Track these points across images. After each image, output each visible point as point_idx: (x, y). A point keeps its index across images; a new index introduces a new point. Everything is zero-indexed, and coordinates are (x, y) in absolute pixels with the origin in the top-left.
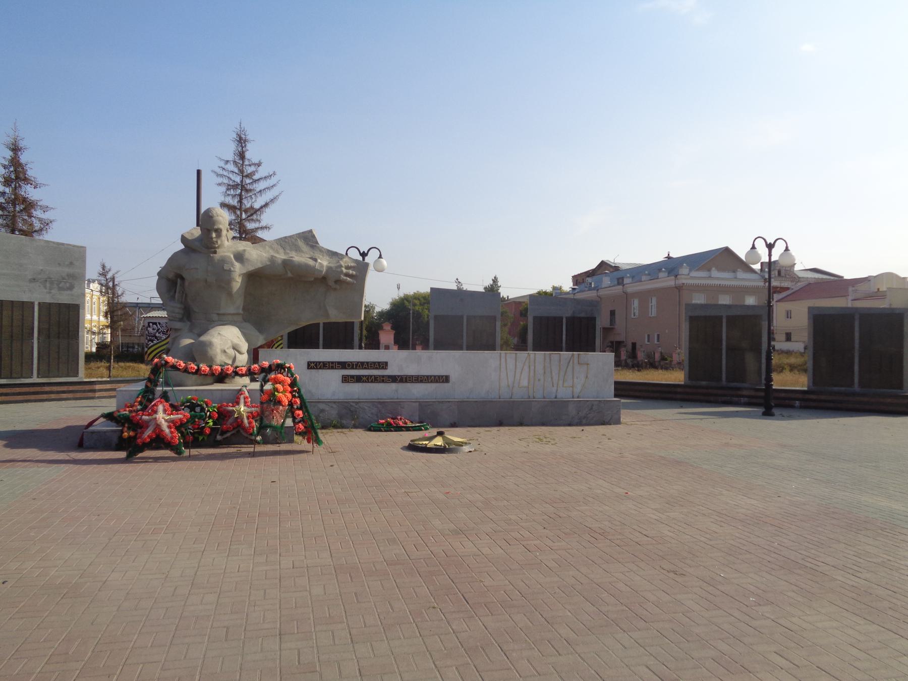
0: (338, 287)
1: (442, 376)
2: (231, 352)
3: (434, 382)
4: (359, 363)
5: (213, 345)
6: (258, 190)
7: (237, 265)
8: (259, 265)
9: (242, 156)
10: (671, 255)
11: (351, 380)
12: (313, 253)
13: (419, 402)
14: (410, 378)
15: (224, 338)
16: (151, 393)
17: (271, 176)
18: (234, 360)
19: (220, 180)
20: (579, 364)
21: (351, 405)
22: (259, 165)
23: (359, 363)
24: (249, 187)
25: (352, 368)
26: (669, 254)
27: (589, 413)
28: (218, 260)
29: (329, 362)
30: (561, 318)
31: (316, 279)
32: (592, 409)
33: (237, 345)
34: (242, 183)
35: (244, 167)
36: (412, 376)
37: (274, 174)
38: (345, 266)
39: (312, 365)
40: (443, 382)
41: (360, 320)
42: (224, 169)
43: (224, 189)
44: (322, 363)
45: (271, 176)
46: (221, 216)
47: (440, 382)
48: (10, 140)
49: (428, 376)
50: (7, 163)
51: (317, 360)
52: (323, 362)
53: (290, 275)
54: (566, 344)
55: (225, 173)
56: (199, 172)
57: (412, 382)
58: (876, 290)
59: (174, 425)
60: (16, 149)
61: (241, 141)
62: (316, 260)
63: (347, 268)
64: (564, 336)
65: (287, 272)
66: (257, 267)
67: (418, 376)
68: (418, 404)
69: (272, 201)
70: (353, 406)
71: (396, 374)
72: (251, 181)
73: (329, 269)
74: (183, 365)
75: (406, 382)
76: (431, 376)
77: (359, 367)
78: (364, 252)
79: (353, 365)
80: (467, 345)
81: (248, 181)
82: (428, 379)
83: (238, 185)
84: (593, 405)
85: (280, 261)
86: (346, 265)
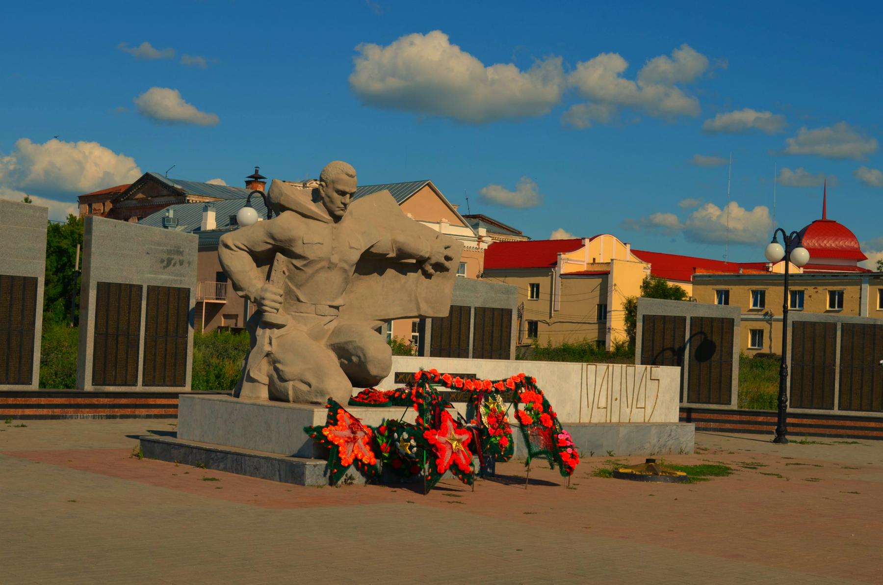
10: (260, 173)
20: (651, 379)
26: (257, 171)
27: (668, 441)
30: (470, 308)
32: (670, 435)
54: (474, 346)
58: (592, 262)
64: (471, 335)
84: (671, 431)
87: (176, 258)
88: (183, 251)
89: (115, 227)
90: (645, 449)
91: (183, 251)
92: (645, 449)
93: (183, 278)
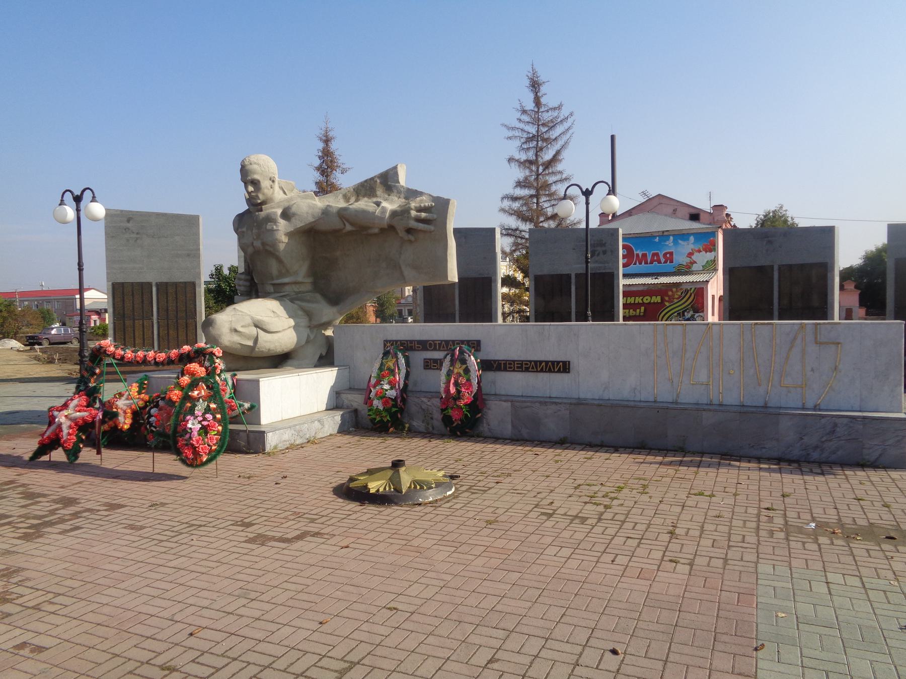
0: (412, 238)
1: (558, 362)
2: (254, 331)
3: (546, 372)
4: (443, 343)
5: (215, 324)
6: (554, 137)
7: (282, 223)
8: (311, 219)
9: (537, 102)
11: (433, 366)
12: (389, 195)
13: (512, 401)
14: (511, 364)
15: (240, 313)
16: (84, 385)
17: (567, 118)
18: (256, 340)
19: (511, 134)
21: (422, 401)
22: (559, 108)
23: (443, 343)
24: (545, 137)
25: (435, 349)
28: (263, 218)
29: (407, 341)
31: (382, 230)
32: (833, 432)
33: (259, 321)
34: (538, 133)
35: (540, 114)
36: (514, 361)
37: (571, 114)
38: (415, 207)
39: (388, 344)
40: (559, 371)
41: (446, 283)
42: (520, 120)
43: (517, 143)
44: (399, 343)
45: (567, 118)
46: (255, 163)
47: (554, 372)
48: (320, 132)
49: (536, 362)
50: (320, 154)
51: (394, 339)
52: (401, 341)
53: (349, 228)
55: (522, 126)
56: (613, 137)
57: (514, 371)
59: (76, 424)
60: (327, 141)
61: (535, 85)
62: (378, 204)
63: (420, 210)
65: (345, 225)
66: (308, 222)
67: (522, 361)
68: (509, 404)
69: (563, 147)
70: (425, 403)
71: (493, 358)
72: (546, 129)
73: (394, 214)
74: (112, 349)
75: (505, 370)
76: (541, 362)
77: (443, 347)
78: (587, 189)
79: (435, 344)
80: (780, 309)
81: (544, 129)
82: (537, 368)
83: (534, 136)
85: (335, 211)
86: (417, 205)
87: (599, 249)
88: (605, 243)
89: (546, 233)
90: (765, 448)
91: (605, 243)
92: (765, 448)
93: (606, 265)
